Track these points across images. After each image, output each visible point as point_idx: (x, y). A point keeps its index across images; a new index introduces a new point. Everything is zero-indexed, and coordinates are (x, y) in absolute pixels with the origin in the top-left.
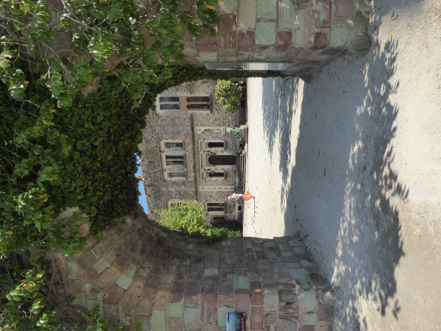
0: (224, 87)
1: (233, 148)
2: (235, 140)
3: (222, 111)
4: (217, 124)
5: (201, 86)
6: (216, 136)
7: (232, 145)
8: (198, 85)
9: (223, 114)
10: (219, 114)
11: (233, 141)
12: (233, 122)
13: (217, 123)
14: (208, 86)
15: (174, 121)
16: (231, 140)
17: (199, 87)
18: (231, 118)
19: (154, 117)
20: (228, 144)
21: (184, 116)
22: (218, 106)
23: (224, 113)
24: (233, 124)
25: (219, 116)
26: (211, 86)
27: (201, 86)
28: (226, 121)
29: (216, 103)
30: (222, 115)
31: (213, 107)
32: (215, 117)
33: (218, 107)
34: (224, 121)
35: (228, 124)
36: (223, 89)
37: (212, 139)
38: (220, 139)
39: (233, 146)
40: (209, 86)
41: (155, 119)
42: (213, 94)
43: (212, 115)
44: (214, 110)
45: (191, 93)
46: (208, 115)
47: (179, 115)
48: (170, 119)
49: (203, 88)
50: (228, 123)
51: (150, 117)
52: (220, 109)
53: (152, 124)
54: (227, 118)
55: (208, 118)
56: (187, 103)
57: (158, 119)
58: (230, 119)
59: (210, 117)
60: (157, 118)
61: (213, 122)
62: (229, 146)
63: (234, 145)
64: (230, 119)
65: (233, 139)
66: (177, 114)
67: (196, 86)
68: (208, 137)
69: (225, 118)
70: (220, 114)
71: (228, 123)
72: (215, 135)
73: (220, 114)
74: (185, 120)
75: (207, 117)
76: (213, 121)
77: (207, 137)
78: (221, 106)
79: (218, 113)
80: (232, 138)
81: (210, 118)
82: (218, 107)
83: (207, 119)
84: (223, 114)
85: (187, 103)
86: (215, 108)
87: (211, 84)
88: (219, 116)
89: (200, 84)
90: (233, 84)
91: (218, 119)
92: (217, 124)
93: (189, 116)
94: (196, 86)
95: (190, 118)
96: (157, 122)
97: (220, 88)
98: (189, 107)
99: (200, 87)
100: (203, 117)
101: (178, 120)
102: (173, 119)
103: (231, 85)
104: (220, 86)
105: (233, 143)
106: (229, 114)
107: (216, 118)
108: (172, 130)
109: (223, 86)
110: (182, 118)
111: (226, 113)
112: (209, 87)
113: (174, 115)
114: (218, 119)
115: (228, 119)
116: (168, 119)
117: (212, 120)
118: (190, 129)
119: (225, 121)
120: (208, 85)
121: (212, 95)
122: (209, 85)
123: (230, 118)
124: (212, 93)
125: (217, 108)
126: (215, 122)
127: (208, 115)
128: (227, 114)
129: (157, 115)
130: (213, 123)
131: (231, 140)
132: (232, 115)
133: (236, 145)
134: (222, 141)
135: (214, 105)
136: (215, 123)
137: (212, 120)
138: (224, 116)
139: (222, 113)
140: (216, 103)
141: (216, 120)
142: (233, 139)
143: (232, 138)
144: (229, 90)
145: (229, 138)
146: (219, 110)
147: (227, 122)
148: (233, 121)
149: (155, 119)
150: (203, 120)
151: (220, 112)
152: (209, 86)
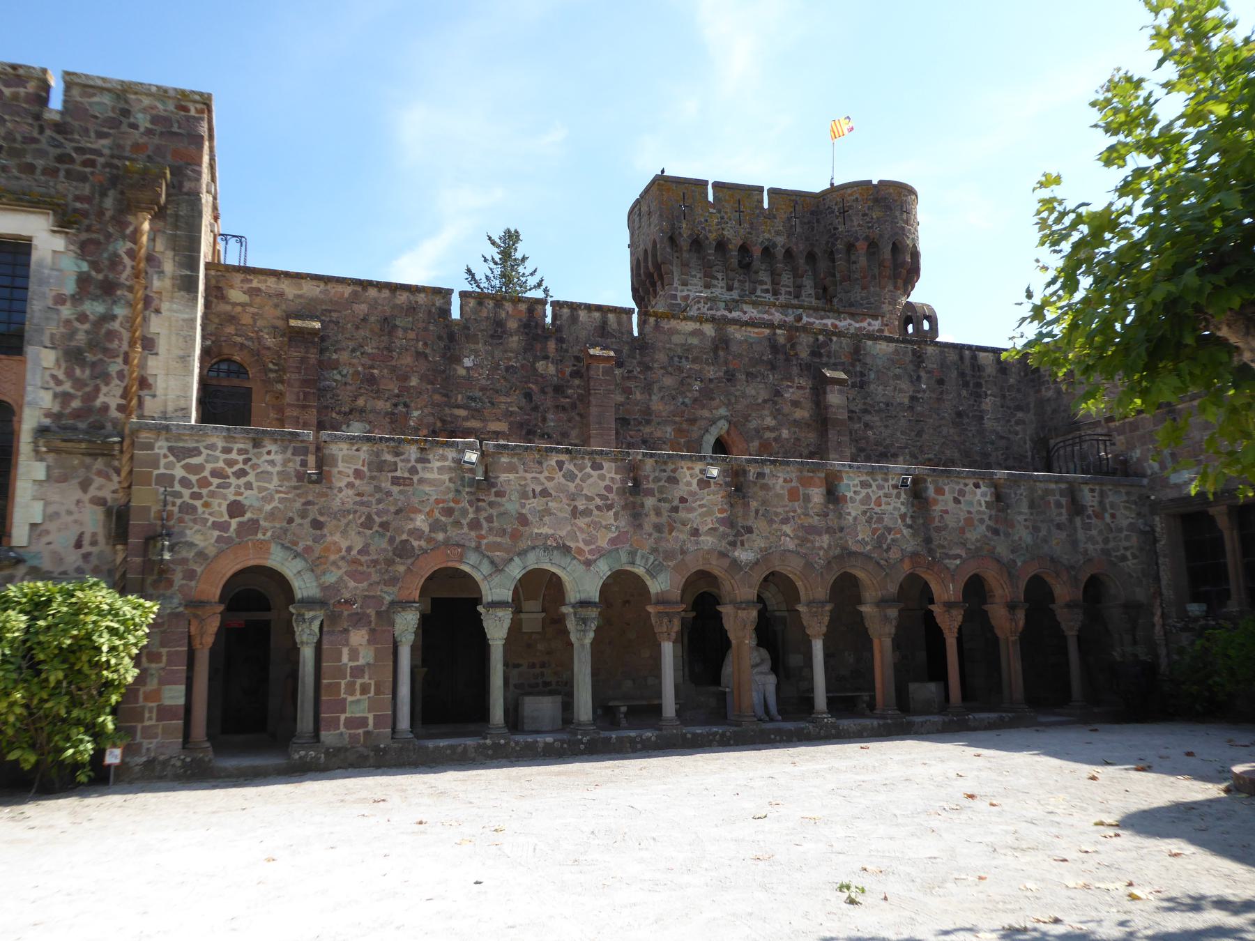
0: (104, 641)
5: (86, 498)
8: (98, 481)
14: (87, 540)
17: (85, 486)
26: (86, 557)
27: (86, 498)
36: (89, 636)
40: (87, 548)
42: (22, 569)
45: (41, 431)
49: (69, 513)
67: (88, 468)
87: (94, 561)
89: (100, 494)
90: (114, 698)
94: (88, 468)
97: (101, 613)
99: (78, 494)
103: (108, 684)
104: (113, 612)
109: (113, 632)
112: (78, 545)
120: (94, 543)
121: (19, 561)
122: (94, 550)
124: (35, 563)
144: (74, 674)
152: (87, 548)
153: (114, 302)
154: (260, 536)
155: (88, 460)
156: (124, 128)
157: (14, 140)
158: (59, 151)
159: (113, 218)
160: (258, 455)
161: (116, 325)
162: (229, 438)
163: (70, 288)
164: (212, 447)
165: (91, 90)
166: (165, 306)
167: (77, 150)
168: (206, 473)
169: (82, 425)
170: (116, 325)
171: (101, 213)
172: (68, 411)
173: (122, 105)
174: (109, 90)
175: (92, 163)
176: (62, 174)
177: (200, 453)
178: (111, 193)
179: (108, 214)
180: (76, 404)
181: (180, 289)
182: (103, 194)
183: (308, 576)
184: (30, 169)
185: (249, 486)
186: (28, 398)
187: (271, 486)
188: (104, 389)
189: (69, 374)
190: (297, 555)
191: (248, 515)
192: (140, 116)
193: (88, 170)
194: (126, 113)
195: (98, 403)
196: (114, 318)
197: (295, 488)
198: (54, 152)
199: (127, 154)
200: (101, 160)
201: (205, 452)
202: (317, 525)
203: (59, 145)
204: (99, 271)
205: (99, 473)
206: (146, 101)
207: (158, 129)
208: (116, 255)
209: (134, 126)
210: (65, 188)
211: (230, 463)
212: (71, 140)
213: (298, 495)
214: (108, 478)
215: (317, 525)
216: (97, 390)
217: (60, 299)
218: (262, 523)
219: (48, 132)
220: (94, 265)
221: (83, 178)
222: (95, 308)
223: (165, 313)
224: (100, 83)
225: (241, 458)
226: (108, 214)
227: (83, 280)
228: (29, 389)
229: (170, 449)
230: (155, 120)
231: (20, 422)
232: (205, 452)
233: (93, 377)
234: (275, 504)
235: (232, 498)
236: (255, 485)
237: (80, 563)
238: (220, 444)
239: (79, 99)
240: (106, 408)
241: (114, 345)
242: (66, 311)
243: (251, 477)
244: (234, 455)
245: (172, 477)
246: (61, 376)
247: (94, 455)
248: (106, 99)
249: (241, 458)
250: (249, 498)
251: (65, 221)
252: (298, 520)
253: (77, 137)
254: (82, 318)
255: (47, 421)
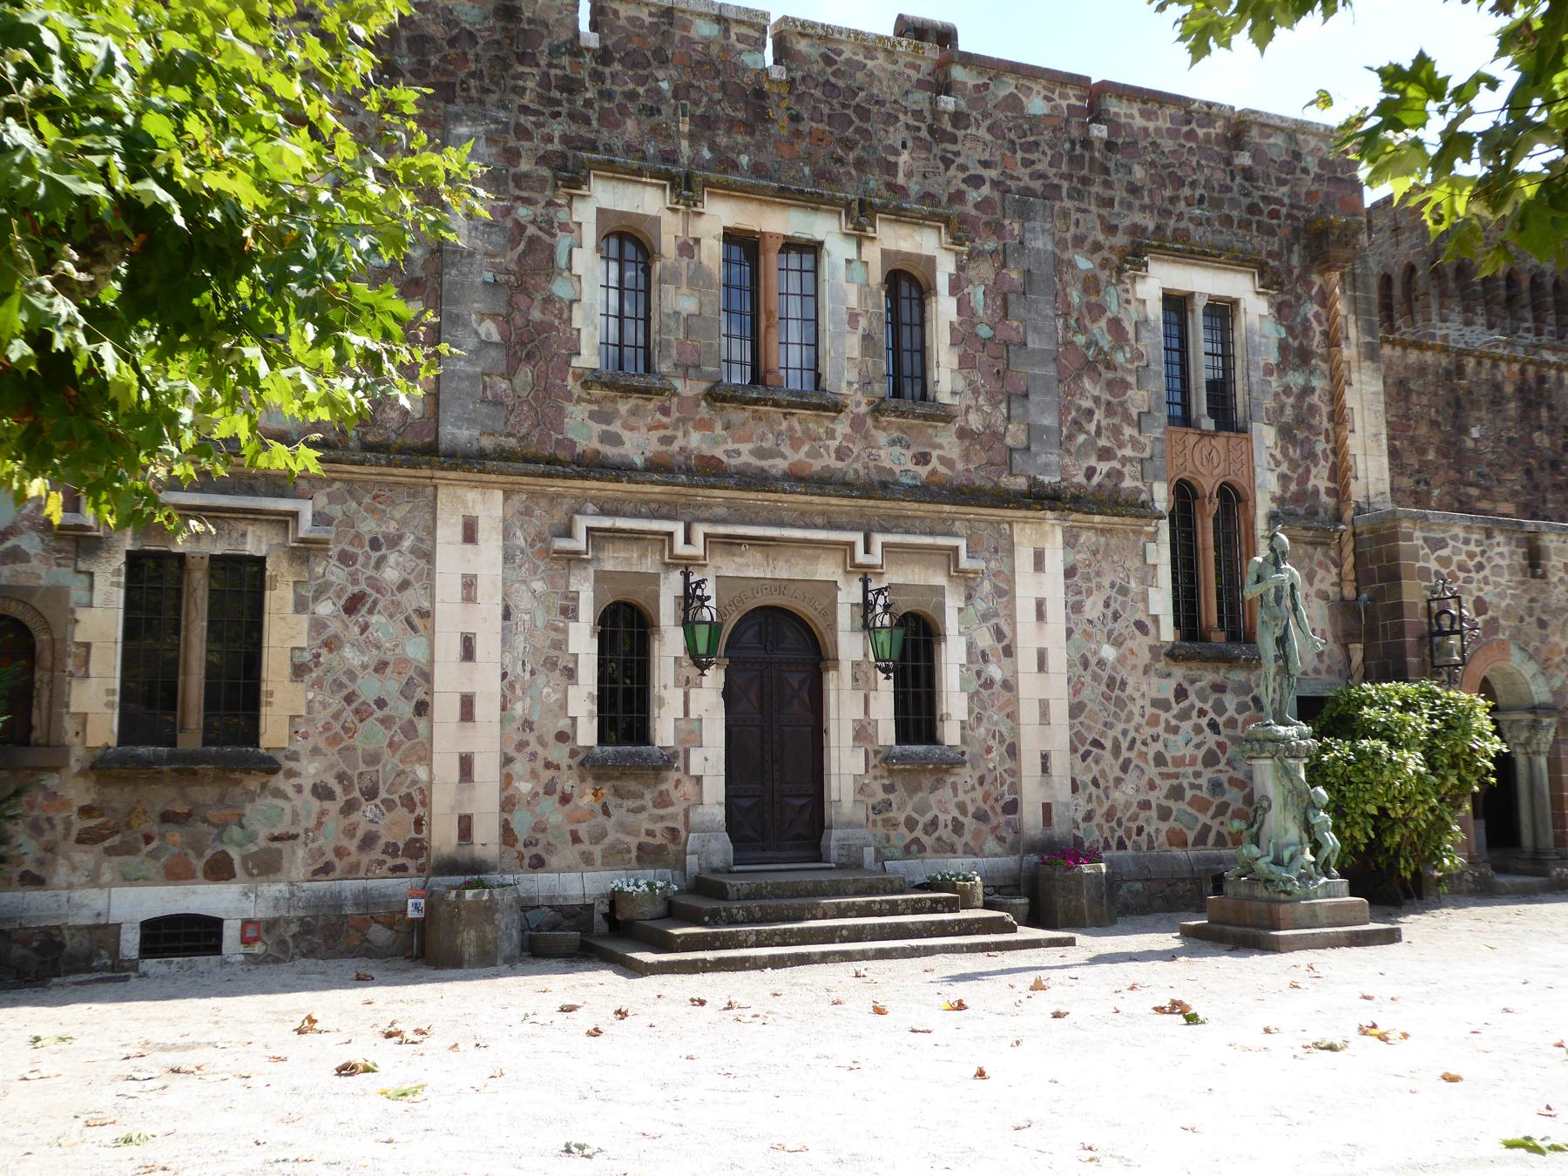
1: (891, 824)
2: (967, 837)
3: (1175, 730)
4: (1086, 694)
5: (1312, 591)
6: (989, 684)
7: (924, 820)
8: (1321, 573)
9: (1155, 739)
10: (1149, 710)
11: (958, 827)
12: (1098, 819)
13: (1092, 693)
15: (1090, 367)
16: (962, 808)
18: (1127, 806)
19: (1111, 229)
20: (927, 781)
21: (1128, 452)
22: (1207, 707)
23: (1159, 746)
24: (1089, 817)
25: (1136, 710)
28: (1102, 765)
29: (1219, 688)
30: (1148, 731)
31: (1195, 669)
32: (1131, 681)
33: (1198, 704)
34: (1108, 744)
35: (1088, 778)
37: (970, 646)
38: (970, 712)
39: (911, 824)
41: (1101, 238)
43: (1145, 657)
44: (1179, 672)
46: (1140, 626)
47: (1134, 412)
48: (1106, 342)
50: (1095, 782)
51: (1110, 203)
52: (1184, 715)
53: (1068, 204)
54: (1125, 767)
55: (1119, 626)
56: (1208, 485)
57: (1098, 257)
58: (1117, 795)
59: (1129, 644)
60: (1105, 253)
61: (1093, 661)
62: (914, 790)
63: (918, 833)
64: (1117, 795)
65: (968, 821)
66: (1138, 399)
67: (1311, 558)
68: (985, 617)
69: (1125, 754)
70: (1154, 721)
71: (1095, 782)
72: (995, 671)
73: (1154, 721)
74: (1105, 454)
75: (1129, 616)
76: (1101, 663)
77: (981, 606)
78: (1204, 722)
79: (1156, 703)
80: (981, 817)
81: (1117, 643)
82: (1198, 704)
83: (1116, 617)
84: (1155, 739)
85: (1208, 485)
86: (1193, 682)
88: (1136, 710)
91: (1120, 703)
92: (1086, 694)
93: (1127, 483)
95: (1117, 489)
96: (1079, 241)
98: (1185, 493)
100: (1123, 591)
101: (1097, 400)
102: (1110, 366)
105: (934, 823)
106: (1152, 786)
107: (1123, 684)
108: (1034, 342)
110: (1116, 431)
111: (1160, 760)
113: (1132, 379)
114: (1120, 703)
115: (1118, 781)
116: (1099, 329)
117: (1109, 652)
118: (1047, 479)
119: (1107, 754)
123: (1126, 794)
125: (1192, 697)
126: (1095, 678)
127: (1140, 626)
128: (1152, 771)
129: (1134, 257)
130: (1086, 665)
131: (962, 808)
132: (1145, 805)
133: (922, 848)
134: (950, 734)
135: (1209, 677)
136: (1088, 679)
137: (1109, 652)
138: (1138, 745)
139: (1160, 729)
140: (1219, 688)
141: (1111, 683)
142: (968, 821)
143: (981, 817)
145: (979, 794)
146: (1176, 708)
147: (1096, 770)
148: (1109, 815)
149: (1101, 238)
150: (1106, 582)
151: (1163, 715)
153: (1311, 373)
154: (1501, 636)
155: (1310, 549)
156: (1298, 174)
157: (1213, 189)
158: (1249, 200)
159: (1299, 278)
160: (1491, 546)
161: (1315, 399)
162: (1468, 529)
163: (1273, 358)
164: (1455, 538)
165: (1268, 130)
166: (1355, 377)
167: (1266, 199)
168: (1453, 567)
169: (1301, 511)
170: (1315, 399)
171: (1290, 271)
172: (1288, 495)
173: (1293, 147)
174: (1282, 130)
175: (1274, 214)
176: (1254, 226)
177: (1446, 546)
178: (1296, 248)
179: (1296, 272)
180: (1293, 487)
181: (1366, 359)
182: (1290, 251)
183: (1541, 680)
184: (1227, 221)
185: (1486, 581)
186: (1258, 481)
187: (1502, 581)
188: (1314, 471)
189: (1284, 452)
190: (1531, 657)
191: (1490, 613)
192: (1309, 159)
193: (1275, 222)
194: (1297, 156)
195: (1310, 485)
196: (1313, 390)
197: (1522, 583)
198: (1246, 201)
199: (1303, 203)
200: (1284, 211)
201: (1451, 543)
202: (1542, 624)
203: (1247, 195)
204: (1295, 338)
205: (1320, 564)
206: (1313, 142)
207: (1327, 175)
208: (1306, 320)
209: (1305, 171)
210: (1263, 245)
211: (1471, 555)
212: (1257, 188)
213: (1525, 591)
214: (1328, 570)
215: (1542, 624)
216: (1308, 471)
217: (1268, 371)
218: (1502, 622)
219: (1238, 179)
220: (1290, 329)
221: (1271, 232)
222: (1296, 379)
223: (1356, 385)
224: (1278, 122)
225: (1478, 550)
226: (1296, 272)
227: (1283, 347)
228: (1258, 470)
229: (1426, 540)
230: (1323, 163)
231: (1255, 507)
232: (1451, 543)
233: (1304, 458)
234: (1508, 601)
235: (1476, 594)
236: (1491, 579)
237: (1316, 662)
238: (1462, 535)
239: (1258, 140)
240: (1316, 491)
241: (1315, 422)
242: (1275, 383)
243: (1487, 572)
244: (1472, 547)
245: (1428, 569)
246: (1279, 457)
247: (1314, 544)
248: (1278, 140)
249: (1478, 550)
250: (1488, 594)
251: (1270, 280)
252: (1528, 619)
253: (1261, 184)
254: (1287, 390)
255: (1274, 506)
